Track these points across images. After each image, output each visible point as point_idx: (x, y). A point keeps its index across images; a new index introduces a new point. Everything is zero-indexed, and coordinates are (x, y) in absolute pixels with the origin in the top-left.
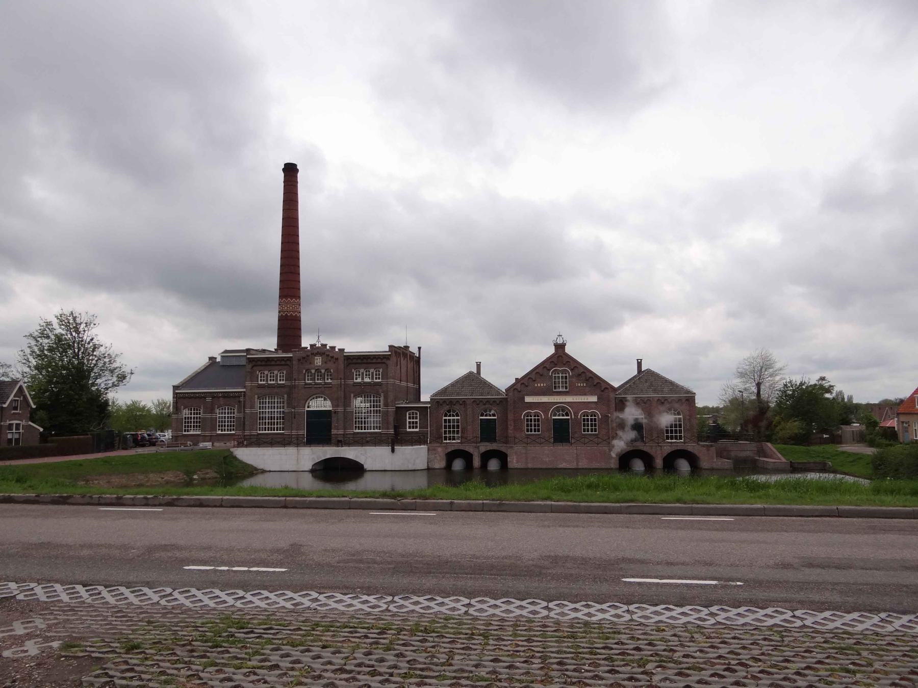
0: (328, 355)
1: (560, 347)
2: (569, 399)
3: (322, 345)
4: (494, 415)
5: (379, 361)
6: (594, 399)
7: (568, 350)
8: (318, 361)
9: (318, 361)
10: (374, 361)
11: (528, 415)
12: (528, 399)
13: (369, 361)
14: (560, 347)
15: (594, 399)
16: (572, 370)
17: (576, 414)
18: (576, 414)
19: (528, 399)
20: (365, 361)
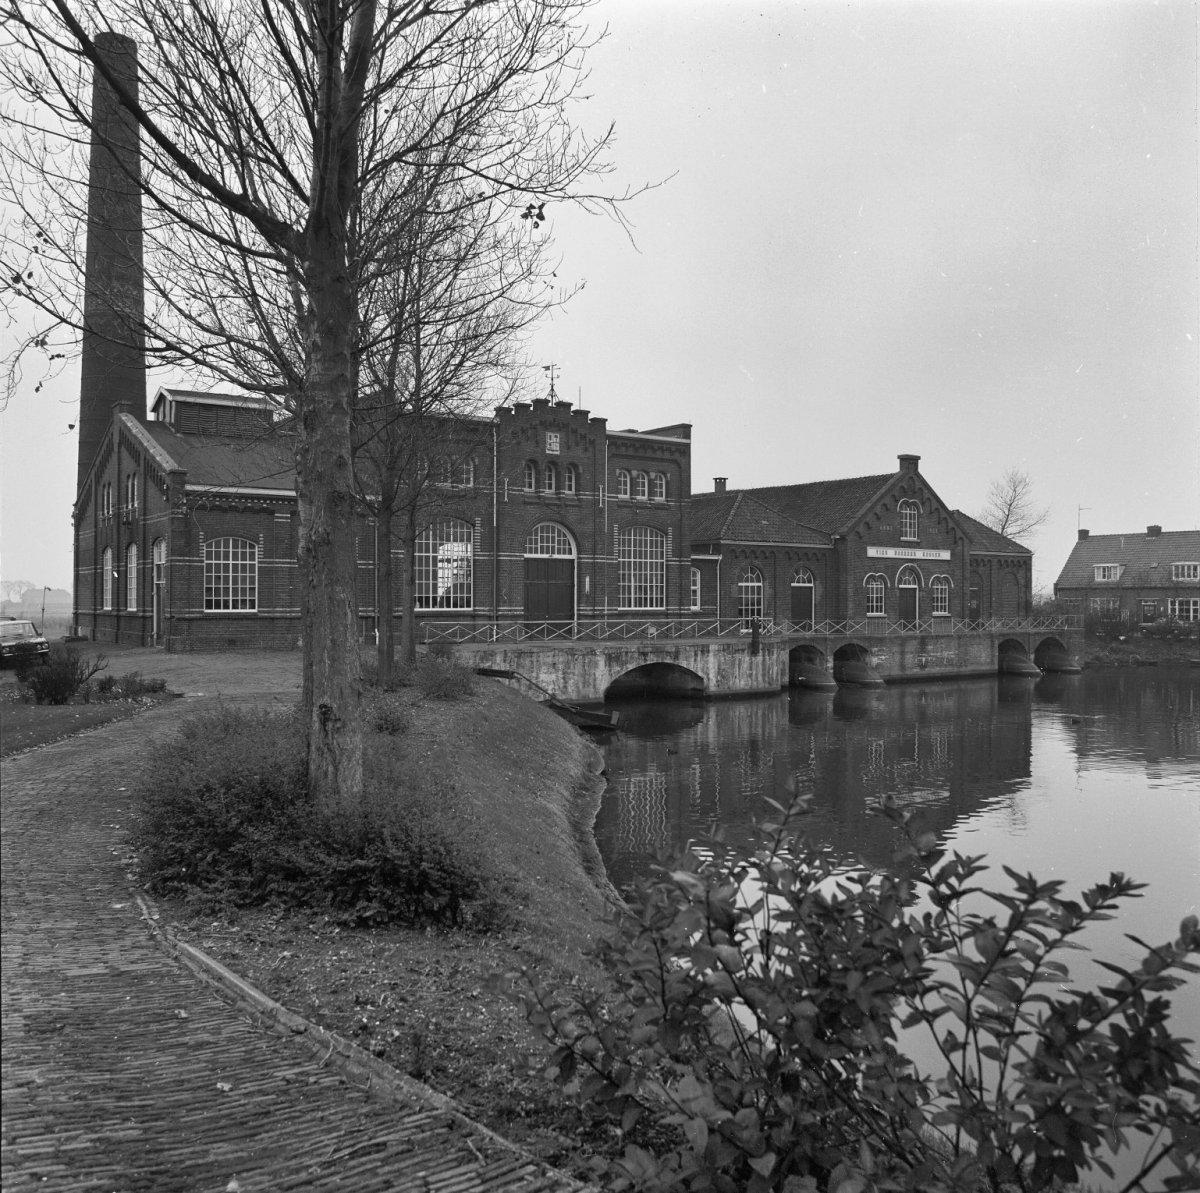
0: (575, 432)
1: (909, 462)
2: (919, 554)
3: (560, 404)
4: (810, 582)
5: (667, 455)
6: (946, 555)
7: (923, 469)
8: (553, 444)
9: (553, 444)
10: (659, 454)
11: (868, 582)
12: (872, 552)
13: (649, 454)
14: (909, 462)
15: (946, 555)
16: (923, 504)
17: (926, 584)
18: (926, 584)
19: (872, 552)
20: (641, 453)
